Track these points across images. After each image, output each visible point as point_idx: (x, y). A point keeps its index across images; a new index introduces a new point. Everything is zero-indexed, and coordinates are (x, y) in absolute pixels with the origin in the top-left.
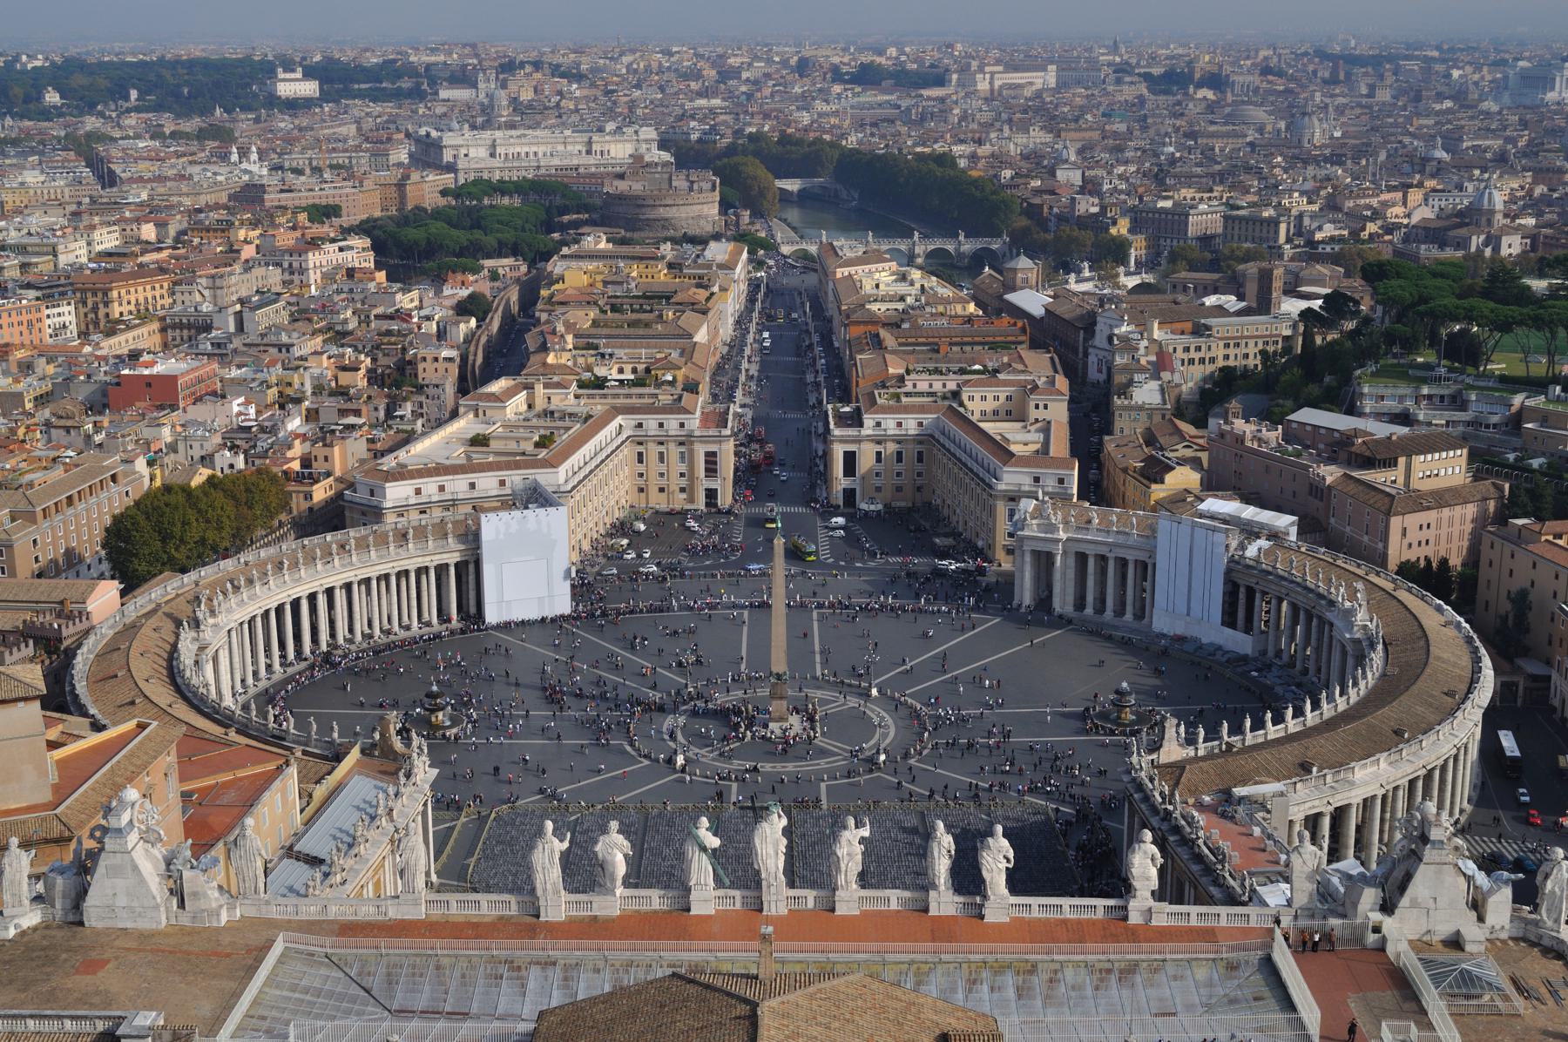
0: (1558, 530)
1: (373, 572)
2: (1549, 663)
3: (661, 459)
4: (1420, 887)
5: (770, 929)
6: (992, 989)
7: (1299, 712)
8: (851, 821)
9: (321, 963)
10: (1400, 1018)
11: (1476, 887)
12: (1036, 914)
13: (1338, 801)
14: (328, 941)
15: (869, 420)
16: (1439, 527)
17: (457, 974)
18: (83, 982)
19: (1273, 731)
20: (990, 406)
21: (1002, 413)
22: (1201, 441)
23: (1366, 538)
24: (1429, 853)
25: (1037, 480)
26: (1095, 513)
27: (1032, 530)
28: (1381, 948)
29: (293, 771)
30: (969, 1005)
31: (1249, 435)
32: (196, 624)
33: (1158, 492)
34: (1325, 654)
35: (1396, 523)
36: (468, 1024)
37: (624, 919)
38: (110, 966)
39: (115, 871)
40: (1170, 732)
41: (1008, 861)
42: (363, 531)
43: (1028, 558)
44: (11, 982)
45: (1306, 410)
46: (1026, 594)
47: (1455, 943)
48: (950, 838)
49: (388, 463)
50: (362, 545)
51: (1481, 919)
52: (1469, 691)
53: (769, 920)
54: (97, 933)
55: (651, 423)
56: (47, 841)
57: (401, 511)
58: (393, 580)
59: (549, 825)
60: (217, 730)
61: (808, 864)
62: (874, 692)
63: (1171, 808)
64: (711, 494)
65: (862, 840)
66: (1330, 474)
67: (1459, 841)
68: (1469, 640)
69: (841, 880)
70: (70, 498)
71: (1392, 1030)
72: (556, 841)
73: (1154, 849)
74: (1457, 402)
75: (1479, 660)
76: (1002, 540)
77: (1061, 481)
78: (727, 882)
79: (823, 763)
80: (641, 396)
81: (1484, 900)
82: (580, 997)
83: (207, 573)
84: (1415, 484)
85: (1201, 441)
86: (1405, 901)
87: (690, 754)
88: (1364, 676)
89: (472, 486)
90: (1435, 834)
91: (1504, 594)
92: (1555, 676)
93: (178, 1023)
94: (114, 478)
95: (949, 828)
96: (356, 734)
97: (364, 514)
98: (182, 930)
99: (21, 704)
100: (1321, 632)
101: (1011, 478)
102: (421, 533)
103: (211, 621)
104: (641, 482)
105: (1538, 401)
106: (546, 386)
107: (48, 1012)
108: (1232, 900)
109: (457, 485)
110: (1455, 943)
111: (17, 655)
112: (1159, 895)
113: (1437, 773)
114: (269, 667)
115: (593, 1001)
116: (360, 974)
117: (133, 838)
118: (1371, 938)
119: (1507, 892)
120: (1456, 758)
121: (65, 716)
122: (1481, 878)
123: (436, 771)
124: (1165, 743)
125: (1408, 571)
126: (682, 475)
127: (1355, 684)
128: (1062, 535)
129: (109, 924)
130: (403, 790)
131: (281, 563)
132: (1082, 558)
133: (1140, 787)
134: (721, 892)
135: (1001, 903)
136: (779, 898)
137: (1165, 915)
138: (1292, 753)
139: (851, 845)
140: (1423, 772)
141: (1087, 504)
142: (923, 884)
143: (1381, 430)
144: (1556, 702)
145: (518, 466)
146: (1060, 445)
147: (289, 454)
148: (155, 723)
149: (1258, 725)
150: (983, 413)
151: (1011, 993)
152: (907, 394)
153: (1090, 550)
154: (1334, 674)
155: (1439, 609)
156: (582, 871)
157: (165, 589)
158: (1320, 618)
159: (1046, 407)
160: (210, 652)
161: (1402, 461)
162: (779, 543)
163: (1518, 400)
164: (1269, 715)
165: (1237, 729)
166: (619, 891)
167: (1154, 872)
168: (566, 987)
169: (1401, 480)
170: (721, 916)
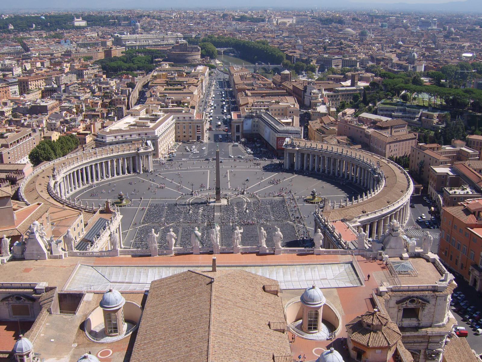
2: (428, 183)
6: (277, 273)
7: (361, 197)
11: (407, 242)
16: (400, 146)
17: (129, 272)
18: (25, 274)
20: (277, 112)
21: (281, 114)
23: (380, 149)
29: (82, 217)
32: (54, 176)
34: (369, 181)
35: (388, 146)
38: (32, 270)
40: (327, 203)
42: (100, 149)
43: (287, 155)
44: (6, 274)
45: (364, 113)
46: (287, 166)
48: (265, 232)
49: (108, 130)
56: (14, 236)
57: (111, 144)
59: (153, 230)
60: (62, 205)
63: (326, 223)
64: (198, 138)
66: (371, 131)
68: (407, 177)
70: (18, 141)
72: (155, 234)
74: (404, 111)
75: (409, 182)
82: (163, 277)
83: (57, 161)
84: (393, 133)
86: (388, 247)
91: (416, 164)
93: (52, 286)
95: (264, 230)
96: (99, 206)
97: (100, 144)
99: (5, 198)
104: (179, 135)
105: (425, 112)
110: (401, 258)
111: (5, 185)
115: (166, 278)
116: (102, 272)
118: (379, 257)
121: (18, 202)
122: (408, 240)
123: (122, 216)
125: (391, 158)
126: (190, 132)
127: (377, 189)
128: (297, 149)
129: (32, 258)
131: (77, 158)
132: (303, 155)
133: (319, 218)
138: (360, 209)
143: (384, 119)
144: (429, 193)
145: (143, 130)
147: (79, 127)
148: (43, 203)
150: (275, 114)
151: (281, 274)
155: (399, 168)
157: (45, 166)
158: (367, 171)
159: (293, 112)
160: (58, 183)
164: (353, 197)
166: (173, 248)
167: (321, 241)
168: (159, 275)
169: (389, 133)
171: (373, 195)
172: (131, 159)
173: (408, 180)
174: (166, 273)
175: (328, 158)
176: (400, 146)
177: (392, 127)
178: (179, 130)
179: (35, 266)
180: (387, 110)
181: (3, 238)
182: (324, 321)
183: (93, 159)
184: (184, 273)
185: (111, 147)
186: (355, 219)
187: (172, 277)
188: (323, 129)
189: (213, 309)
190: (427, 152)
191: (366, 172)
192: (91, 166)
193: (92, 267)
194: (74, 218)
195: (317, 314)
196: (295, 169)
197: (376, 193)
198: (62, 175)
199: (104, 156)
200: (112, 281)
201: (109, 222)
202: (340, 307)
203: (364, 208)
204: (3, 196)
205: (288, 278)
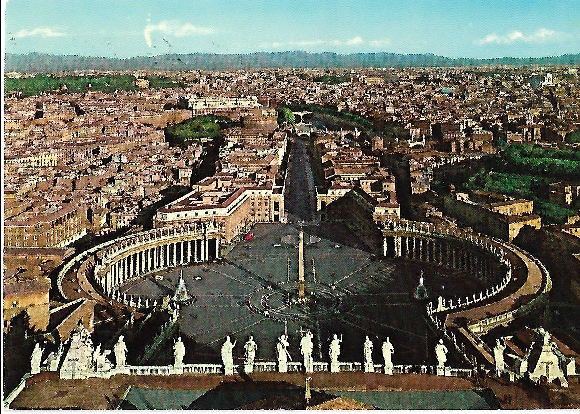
25: (386, 211)
41: (392, 351)
65: (340, 343)
73: (444, 347)
77: (395, 212)
88: (506, 281)
112: (446, 364)
134: (289, 364)
136: (310, 365)
139: (335, 347)
142: (363, 360)
146: (393, 200)
152: (342, 182)
159: (388, 186)
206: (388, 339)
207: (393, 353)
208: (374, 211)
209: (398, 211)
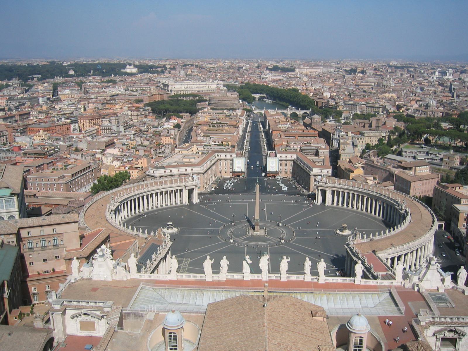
0: (453, 186)
1: (154, 192)
3: (226, 164)
4: (428, 275)
5: (267, 284)
6: (321, 300)
7: (390, 231)
8: (285, 257)
9: (152, 291)
10: (424, 308)
12: (331, 281)
13: (399, 254)
14: (153, 284)
15: (279, 156)
18: (92, 293)
19: (383, 236)
22: (363, 162)
24: (431, 267)
25: (321, 171)
26: (336, 180)
27: (321, 184)
28: (419, 291)
30: (316, 304)
31: (375, 161)
33: (352, 175)
34: (395, 217)
35: (412, 184)
36: (189, 307)
37: (227, 281)
38: (99, 290)
39: (100, 266)
40: (358, 236)
43: (319, 191)
47: (438, 289)
50: (151, 184)
51: (443, 283)
52: (432, 226)
53: (266, 282)
54: (96, 281)
55: (223, 155)
58: (159, 194)
59: (208, 257)
61: (274, 268)
62: (281, 224)
65: (288, 262)
67: (438, 264)
69: (282, 272)
71: (423, 311)
73: (362, 265)
75: (433, 219)
76: (312, 187)
77: (328, 172)
78: (253, 272)
79: (268, 242)
80: (220, 148)
81: (444, 279)
85: (363, 162)
87: (234, 239)
89: (179, 170)
90: (433, 262)
92: (452, 224)
94: (89, 167)
95: (310, 260)
98: (117, 281)
100: (394, 212)
101: (316, 171)
102: (166, 182)
103: (115, 203)
106: (196, 145)
107: (85, 301)
108: (375, 278)
109: (175, 171)
110: (438, 289)
112: (362, 277)
113: (423, 247)
114: (128, 216)
116: (161, 293)
117: (105, 257)
118: (416, 289)
119: (450, 277)
120: (428, 243)
122: (443, 273)
124: (357, 239)
128: (328, 185)
130: (164, 247)
132: (333, 192)
134: (252, 275)
135: (323, 279)
137: (364, 282)
139: (284, 264)
140: (420, 247)
141: (334, 178)
142: (304, 274)
144: (452, 229)
145: (188, 166)
149: (380, 234)
153: (335, 189)
154: (397, 222)
155: (424, 206)
156: (216, 269)
161: (414, 168)
162: (258, 186)
163: (443, 154)
164: (382, 232)
165: (374, 235)
170: (252, 281)
171: (400, 231)
172: (179, 191)
173: (433, 217)
174: (220, 296)
175: (357, 195)
176: (423, 184)
177: (415, 167)
178: (221, 167)
179: (101, 286)
180: (411, 152)
181: (73, 259)
182: (367, 347)
183: (145, 190)
184: (238, 298)
185: (161, 180)
186: (384, 251)
187: (226, 300)
188: (352, 168)
189: (267, 332)
190: (450, 191)
191: (392, 208)
192: (143, 197)
193: (153, 289)
194: (131, 243)
195: (361, 340)
196: (326, 204)
197: (403, 229)
198: (118, 204)
199: (154, 188)
200: (172, 301)
201: (161, 247)
202: (383, 334)
203: (393, 242)
204: (71, 221)
205: (332, 305)
206: (322, 260)
207: (326, 269)
208: (312, 171)
209: (330, 172)
